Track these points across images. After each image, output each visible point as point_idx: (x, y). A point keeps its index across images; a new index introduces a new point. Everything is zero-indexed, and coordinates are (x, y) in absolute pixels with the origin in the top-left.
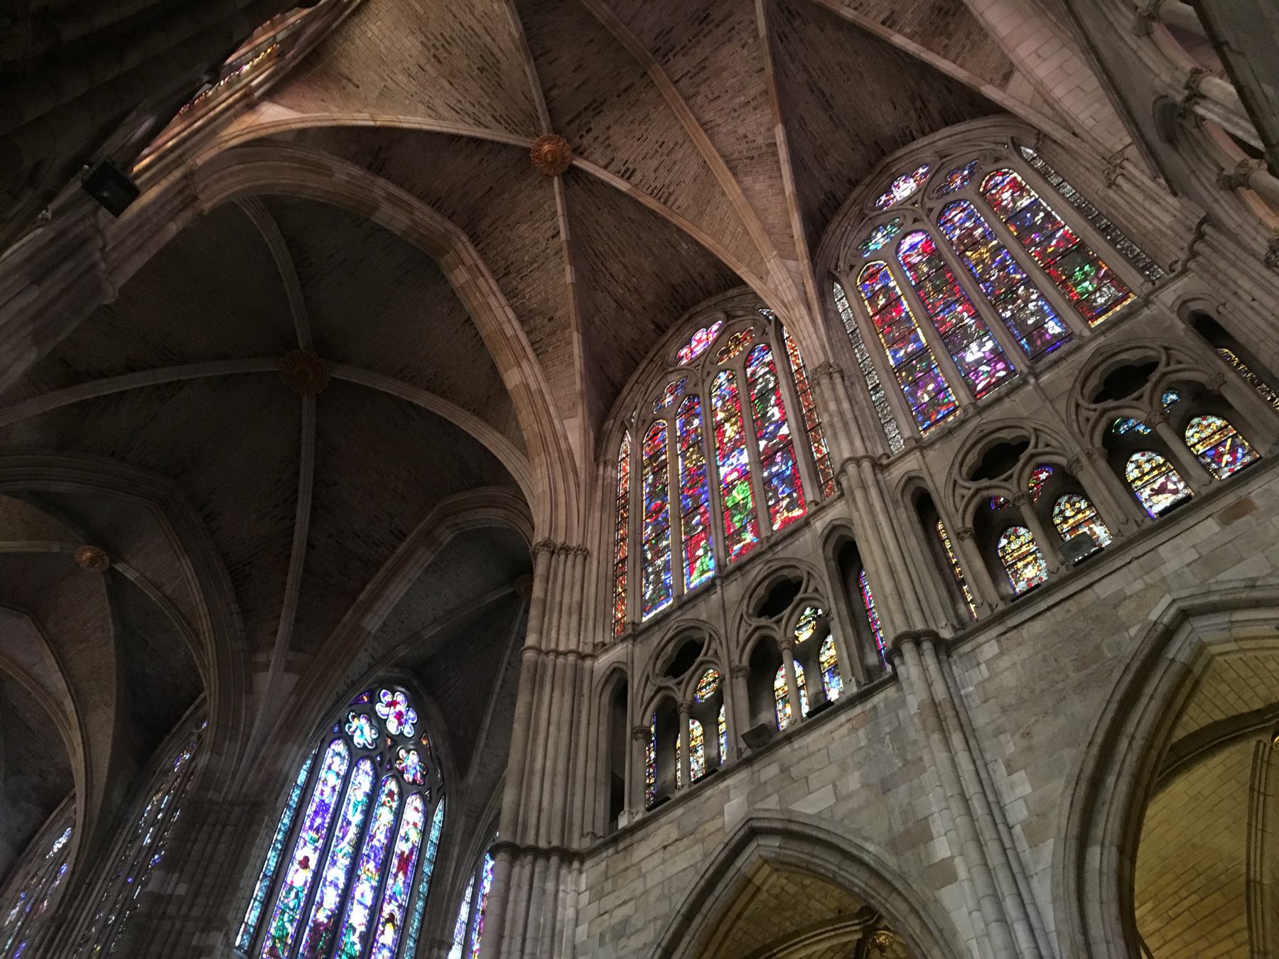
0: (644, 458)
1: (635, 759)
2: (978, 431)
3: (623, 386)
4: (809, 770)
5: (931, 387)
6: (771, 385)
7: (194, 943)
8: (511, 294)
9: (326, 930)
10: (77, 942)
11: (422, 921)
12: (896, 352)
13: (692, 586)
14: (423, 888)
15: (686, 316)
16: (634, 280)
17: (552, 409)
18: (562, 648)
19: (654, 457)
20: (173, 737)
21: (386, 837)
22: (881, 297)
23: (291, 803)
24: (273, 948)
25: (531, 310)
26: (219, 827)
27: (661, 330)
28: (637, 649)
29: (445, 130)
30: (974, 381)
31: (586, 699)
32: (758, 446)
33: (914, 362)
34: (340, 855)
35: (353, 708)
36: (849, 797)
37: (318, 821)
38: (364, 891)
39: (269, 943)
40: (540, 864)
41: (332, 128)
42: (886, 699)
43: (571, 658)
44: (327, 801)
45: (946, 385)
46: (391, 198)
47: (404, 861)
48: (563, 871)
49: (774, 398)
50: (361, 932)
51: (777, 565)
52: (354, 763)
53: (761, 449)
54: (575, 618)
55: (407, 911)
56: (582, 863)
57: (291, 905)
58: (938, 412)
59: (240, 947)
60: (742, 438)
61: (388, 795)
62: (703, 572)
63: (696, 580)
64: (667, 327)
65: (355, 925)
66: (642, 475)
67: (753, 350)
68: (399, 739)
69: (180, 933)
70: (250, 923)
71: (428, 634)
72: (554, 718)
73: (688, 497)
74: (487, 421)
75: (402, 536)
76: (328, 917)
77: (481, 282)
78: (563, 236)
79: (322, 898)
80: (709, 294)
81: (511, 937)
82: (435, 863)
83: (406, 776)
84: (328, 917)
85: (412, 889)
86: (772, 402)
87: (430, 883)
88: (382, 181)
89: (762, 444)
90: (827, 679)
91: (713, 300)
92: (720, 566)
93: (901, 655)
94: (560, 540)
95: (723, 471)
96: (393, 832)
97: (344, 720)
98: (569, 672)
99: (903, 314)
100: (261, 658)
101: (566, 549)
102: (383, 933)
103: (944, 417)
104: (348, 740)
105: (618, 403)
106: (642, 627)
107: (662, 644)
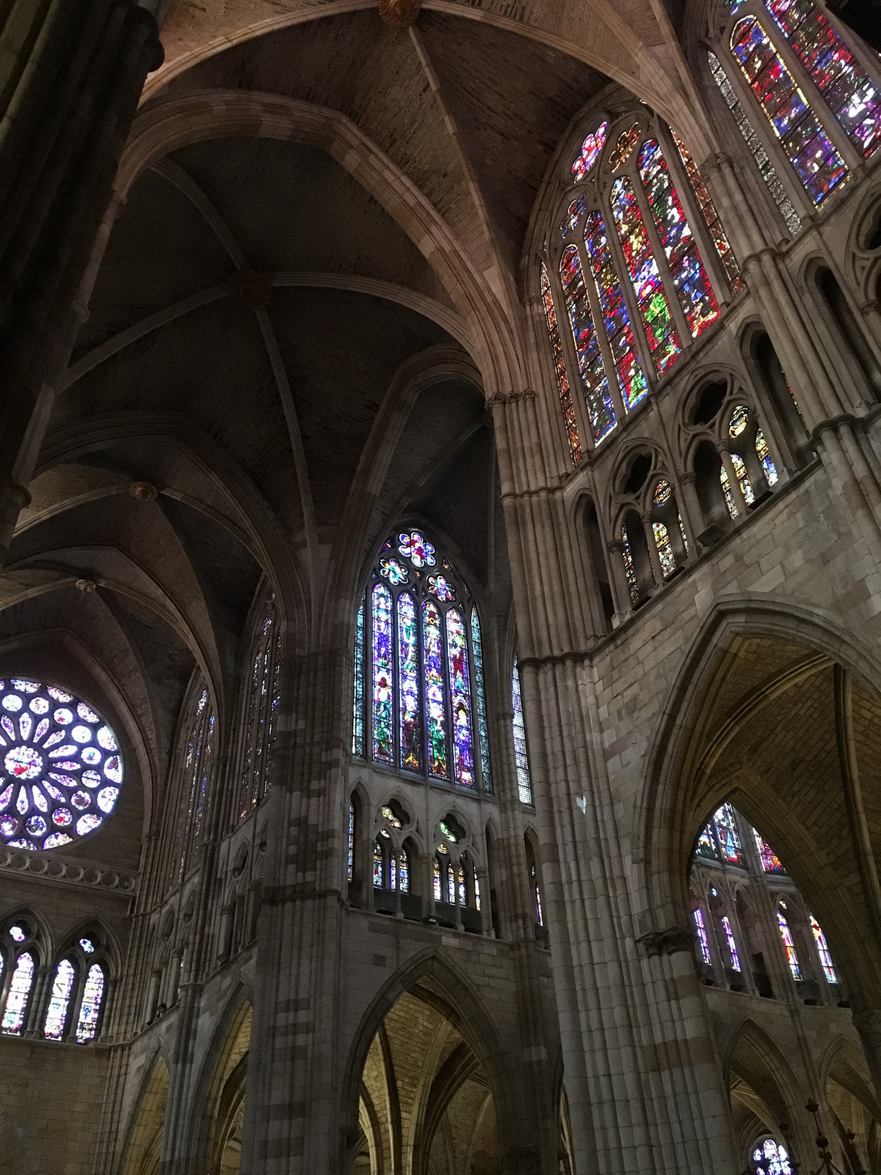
0: (564, 287)
1: (614, 568)
2: (869, 195)
3: (528, 218)
4: (759, 556)
5: (819, 154)
6: (666, 185)
7: (323, 760)
8: (402, 162)
10: (241, 771)
12: (780, 121)
13: (631, 406)
14: (479, 678)
15: (571, 127)
16: (513, 105)
17: (469, 265)
18: (533, 488)
19: (572, 285)
20: (254, 609)
21: (439, 648)
22: (756, 60)
23: (358, 641)
24: (380, 748)
25: (424, 172)
26: (312, 674)
27: (550, 148)
28: (596, 474)
29: (295, 22)
30: (860, 138)
31: (563, 526)
32: (665, 253)
33: (799, 129)
34: (408, 671)
35: (381, 555)
36: (795, 573)
37: (383, 650)
38: (434, 692)
39: (376, 746)
40: (559, 669)
41: (196, 66)
42: (816, 482)
43: (543, 494)
44: (385, 633)
45: (833, 149)
46: (269, 108)
47: (458, 662)
48: (578, 670)
49: (670, 198)
50: (441, 722)
51: (702, 372)
52: (396, 598)
53: (668, 255)
54: (537, 458)
55: (471, 698)
56: (591, 660)
57: (384, 715)
58: (829, 181)
59: (357, 754)
60: (648, 248)
61: (430, 617)
62: (638, 391)
63: (633, 400)
64: (556, 143)
65: (435, 717)
66: (566, 306)
67: (642, 150)
68: (425, 570)
69: (311, 755)
71: (422, 482)
72: (541, 549)
73: (610, 320)
74: (415, 289)
75: (376, 407)
76: (412, 717)
77: (372, 158)
78: (433, 86)
79: (404, 704)
80: (589, 96)
81: (550, 727)
82: (482, 658)
83: (439, 597)
84: (412, 717)
85: (470, 681)
86: (670, 203)
87: (483, 673)
88: (256, 95)
89: (668, 250)
90: (765, 465)
91: (593, 101)
92: (651, 384)
93: (821, 443)
94: (508, 390)
95: (637, 286)
96: (443, 643)
97: (377, 567)
98: (544, 507)
99: (781, 75)
100: (298, 538)
101: (515, 397)
102: (458, 718)
103: (837, 184)
104: (386, 582)
105: (528, 236)
106: (596, 453)
107: (617, 464)
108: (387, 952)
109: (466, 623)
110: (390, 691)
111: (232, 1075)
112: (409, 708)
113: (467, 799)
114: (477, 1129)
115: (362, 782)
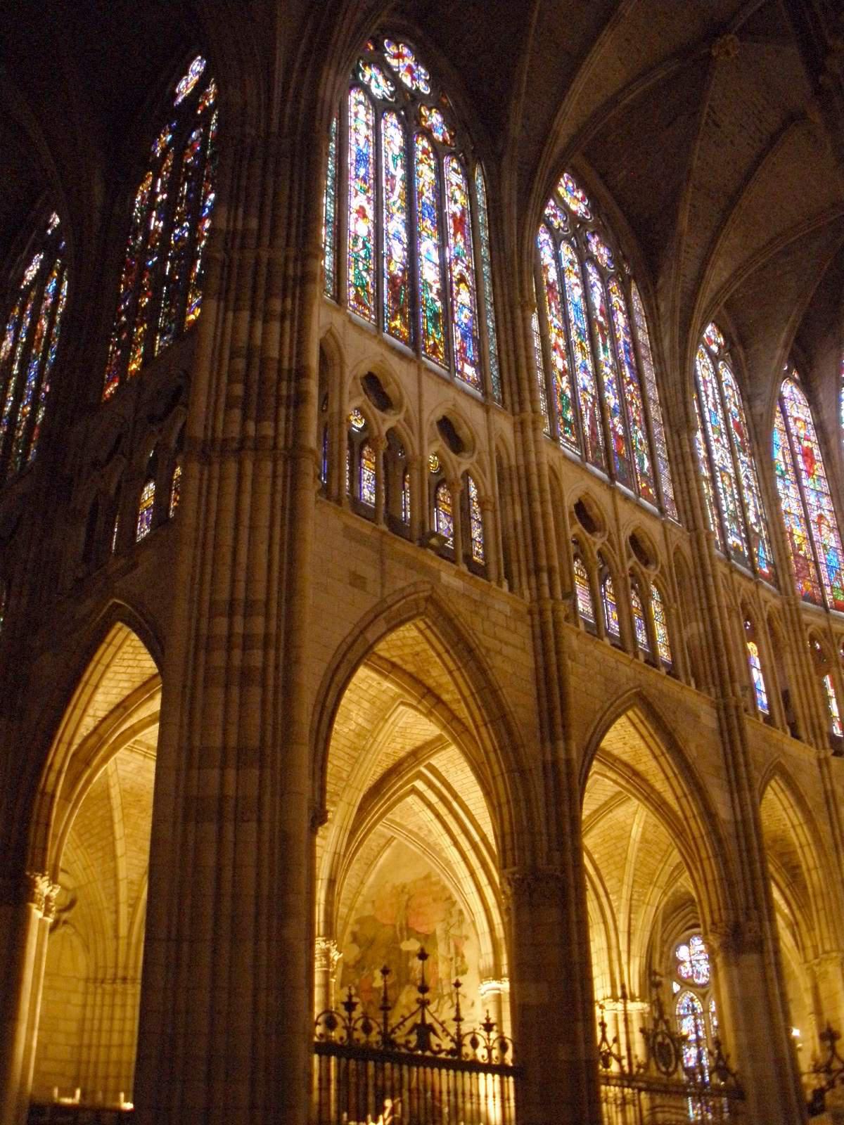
9: (404, 283)
11: (493, 285)
14: (484, 251)
24: (357, 294)
37: (362, 172)
38: (428, 246)
39: (352, 291)
44: (365, 151)
50: (438, 289)
55: (477, 274)
65: (430, 280)
70: (327, 268)
76: (400, 270)
79: (389, 250)
83: (435, 135)
84: (400, 270)
87: (490, 248)
102: (458, 293)
104: (366, 89)
108: (370, 573)
109: (469, 179)
110: (371, 225)
111: (81, 745)
112: (395, 257)
113: (471, 400)
114: (365, 891)
115: (333, 329)
